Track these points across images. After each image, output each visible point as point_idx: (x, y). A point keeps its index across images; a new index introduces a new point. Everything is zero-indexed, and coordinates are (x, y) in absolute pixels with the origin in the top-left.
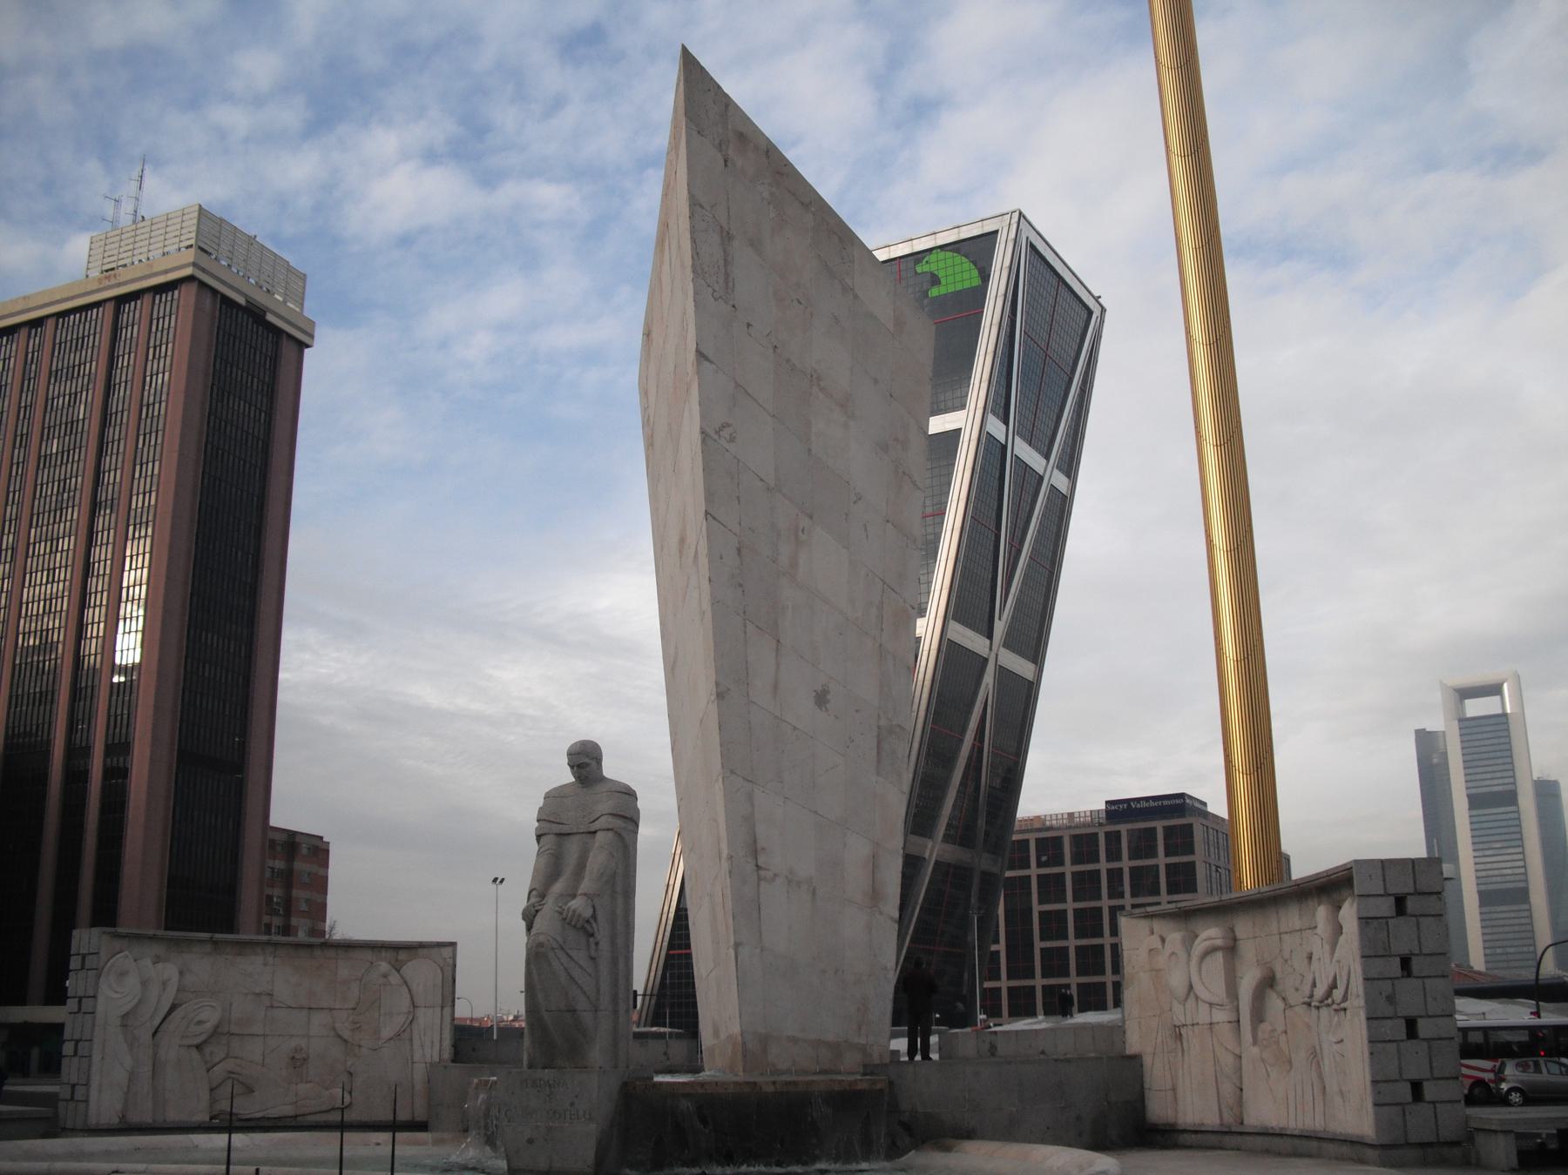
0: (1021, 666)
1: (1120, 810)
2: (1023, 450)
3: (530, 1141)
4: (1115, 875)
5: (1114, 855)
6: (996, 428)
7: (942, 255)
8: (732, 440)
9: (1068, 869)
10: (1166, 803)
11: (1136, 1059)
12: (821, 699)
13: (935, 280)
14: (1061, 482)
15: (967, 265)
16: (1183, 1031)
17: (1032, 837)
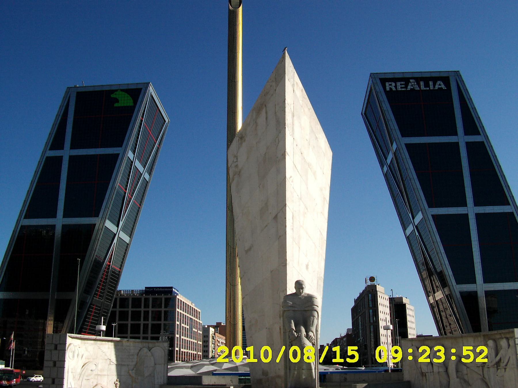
0: (126, 238)
1: (150, 291)
2: (138, 164)
4: (146, 313)
5: (146, 306)
7: (121, 93)
8: (292, 181)
10: (166, 289)
11: (409, 382)
12: (307, 266)
13: (117, 101)
14: (147, 176)
15: (130, 98)
16: (427, 374)
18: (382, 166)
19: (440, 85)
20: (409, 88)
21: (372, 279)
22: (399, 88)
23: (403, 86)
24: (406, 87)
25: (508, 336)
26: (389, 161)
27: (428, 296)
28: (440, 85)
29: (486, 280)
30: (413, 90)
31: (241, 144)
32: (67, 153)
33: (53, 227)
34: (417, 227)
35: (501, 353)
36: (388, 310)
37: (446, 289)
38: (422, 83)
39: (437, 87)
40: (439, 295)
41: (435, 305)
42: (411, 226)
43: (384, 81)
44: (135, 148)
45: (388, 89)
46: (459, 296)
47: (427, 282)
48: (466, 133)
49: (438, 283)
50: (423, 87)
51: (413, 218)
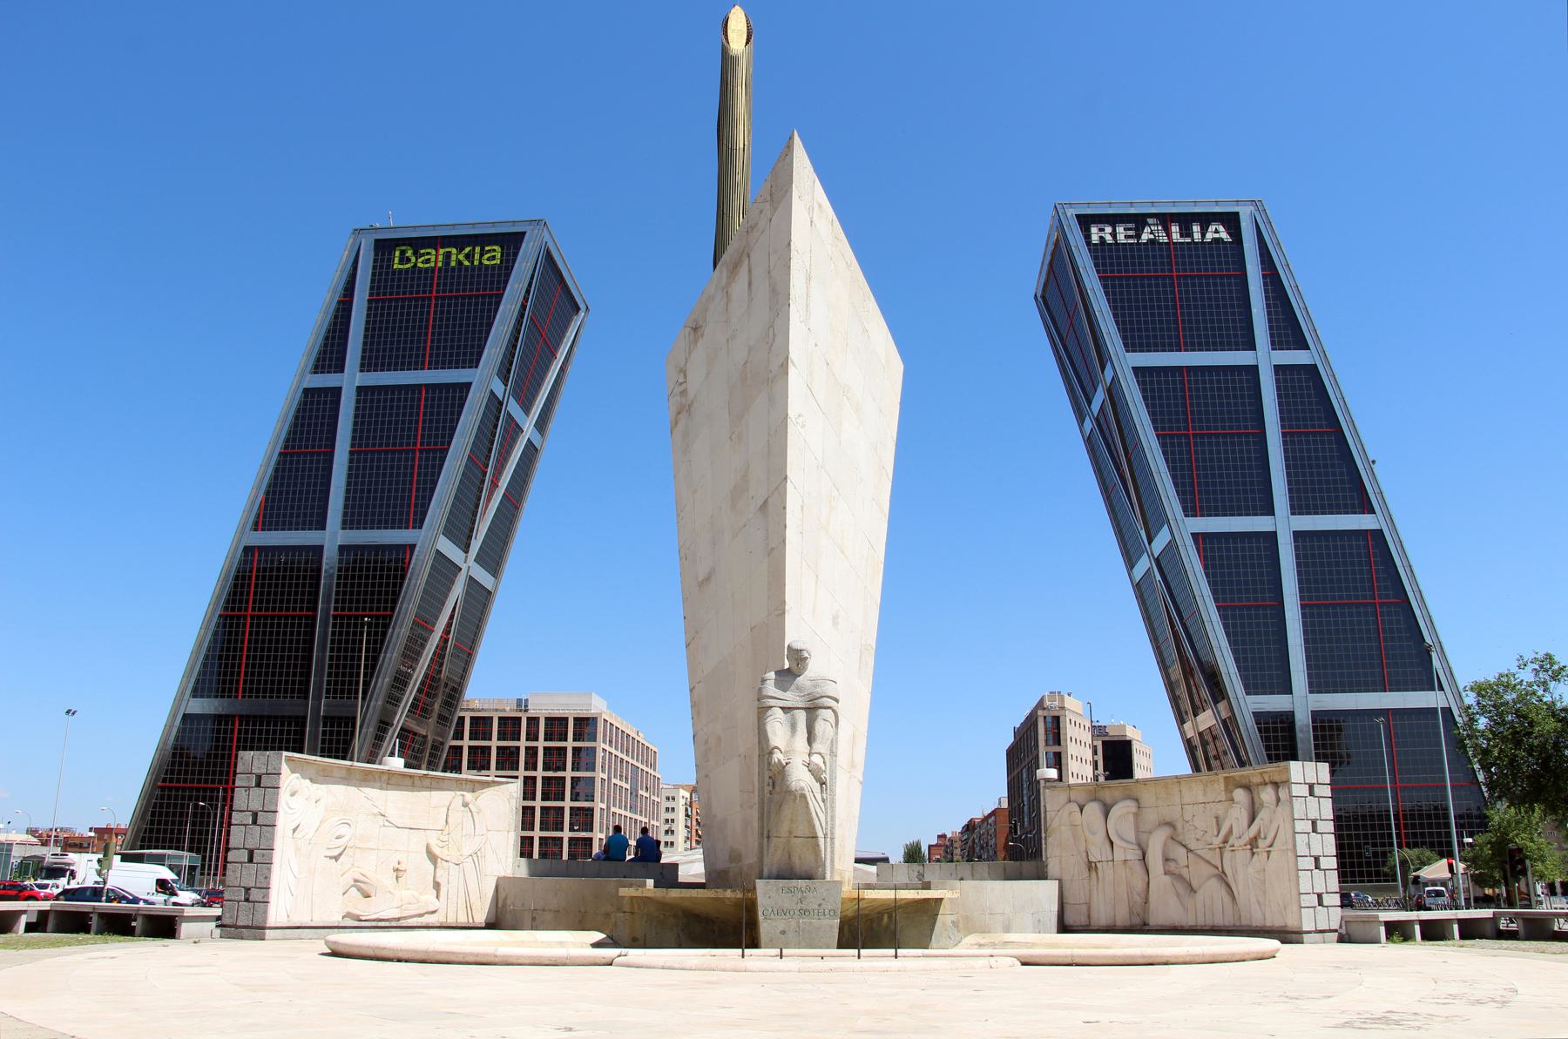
2: (513, 407)
3: (783, 932)
4: (532, 752)
6: (499, 388)
9: (495, 743)
17: (468, 716)
18: (1081, 420)
19: (1217, 231)
20: (1145, 237)
22: (1121, 238)
23: (1131, 233)
24: (1138, 236)
25: (1277, 778)
26: (1096, 407)
27: (1181, 721)
28: (1217, 232)
29: (1316, 686)
30: (1152, 242)
31: (696, 341)
32: (351, 379)
33: (319, 550)
34: (1157, 561)
35: (1263, 815)
36: (1088, 754)
37: (1222, 706)
38: (1175, 229)
39: (1209, 236)
40: (1206, 720)
41: (1197, 742)
43: (1085, 221)
44: (509, 371)
45: (1095, 239)
46: (1251, 721)
47: (1182, 691)
48: (1277, 343)
49: (1205, 693)
50: (1176, 237)
51: (1150, 541)
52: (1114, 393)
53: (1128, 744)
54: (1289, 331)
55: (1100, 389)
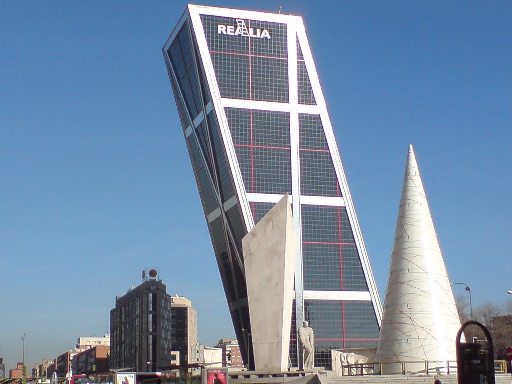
21: (153, 273)
24: (235, 32)
30: (240, 36)
34: (226, 214)
42: (219, 209)
52: (212, 119)
53: (186, 309)
54: (306, 97)
55: (202, 114)
